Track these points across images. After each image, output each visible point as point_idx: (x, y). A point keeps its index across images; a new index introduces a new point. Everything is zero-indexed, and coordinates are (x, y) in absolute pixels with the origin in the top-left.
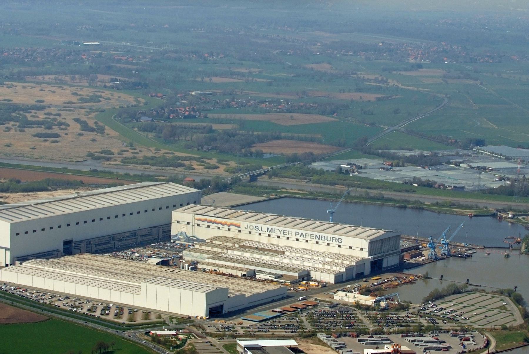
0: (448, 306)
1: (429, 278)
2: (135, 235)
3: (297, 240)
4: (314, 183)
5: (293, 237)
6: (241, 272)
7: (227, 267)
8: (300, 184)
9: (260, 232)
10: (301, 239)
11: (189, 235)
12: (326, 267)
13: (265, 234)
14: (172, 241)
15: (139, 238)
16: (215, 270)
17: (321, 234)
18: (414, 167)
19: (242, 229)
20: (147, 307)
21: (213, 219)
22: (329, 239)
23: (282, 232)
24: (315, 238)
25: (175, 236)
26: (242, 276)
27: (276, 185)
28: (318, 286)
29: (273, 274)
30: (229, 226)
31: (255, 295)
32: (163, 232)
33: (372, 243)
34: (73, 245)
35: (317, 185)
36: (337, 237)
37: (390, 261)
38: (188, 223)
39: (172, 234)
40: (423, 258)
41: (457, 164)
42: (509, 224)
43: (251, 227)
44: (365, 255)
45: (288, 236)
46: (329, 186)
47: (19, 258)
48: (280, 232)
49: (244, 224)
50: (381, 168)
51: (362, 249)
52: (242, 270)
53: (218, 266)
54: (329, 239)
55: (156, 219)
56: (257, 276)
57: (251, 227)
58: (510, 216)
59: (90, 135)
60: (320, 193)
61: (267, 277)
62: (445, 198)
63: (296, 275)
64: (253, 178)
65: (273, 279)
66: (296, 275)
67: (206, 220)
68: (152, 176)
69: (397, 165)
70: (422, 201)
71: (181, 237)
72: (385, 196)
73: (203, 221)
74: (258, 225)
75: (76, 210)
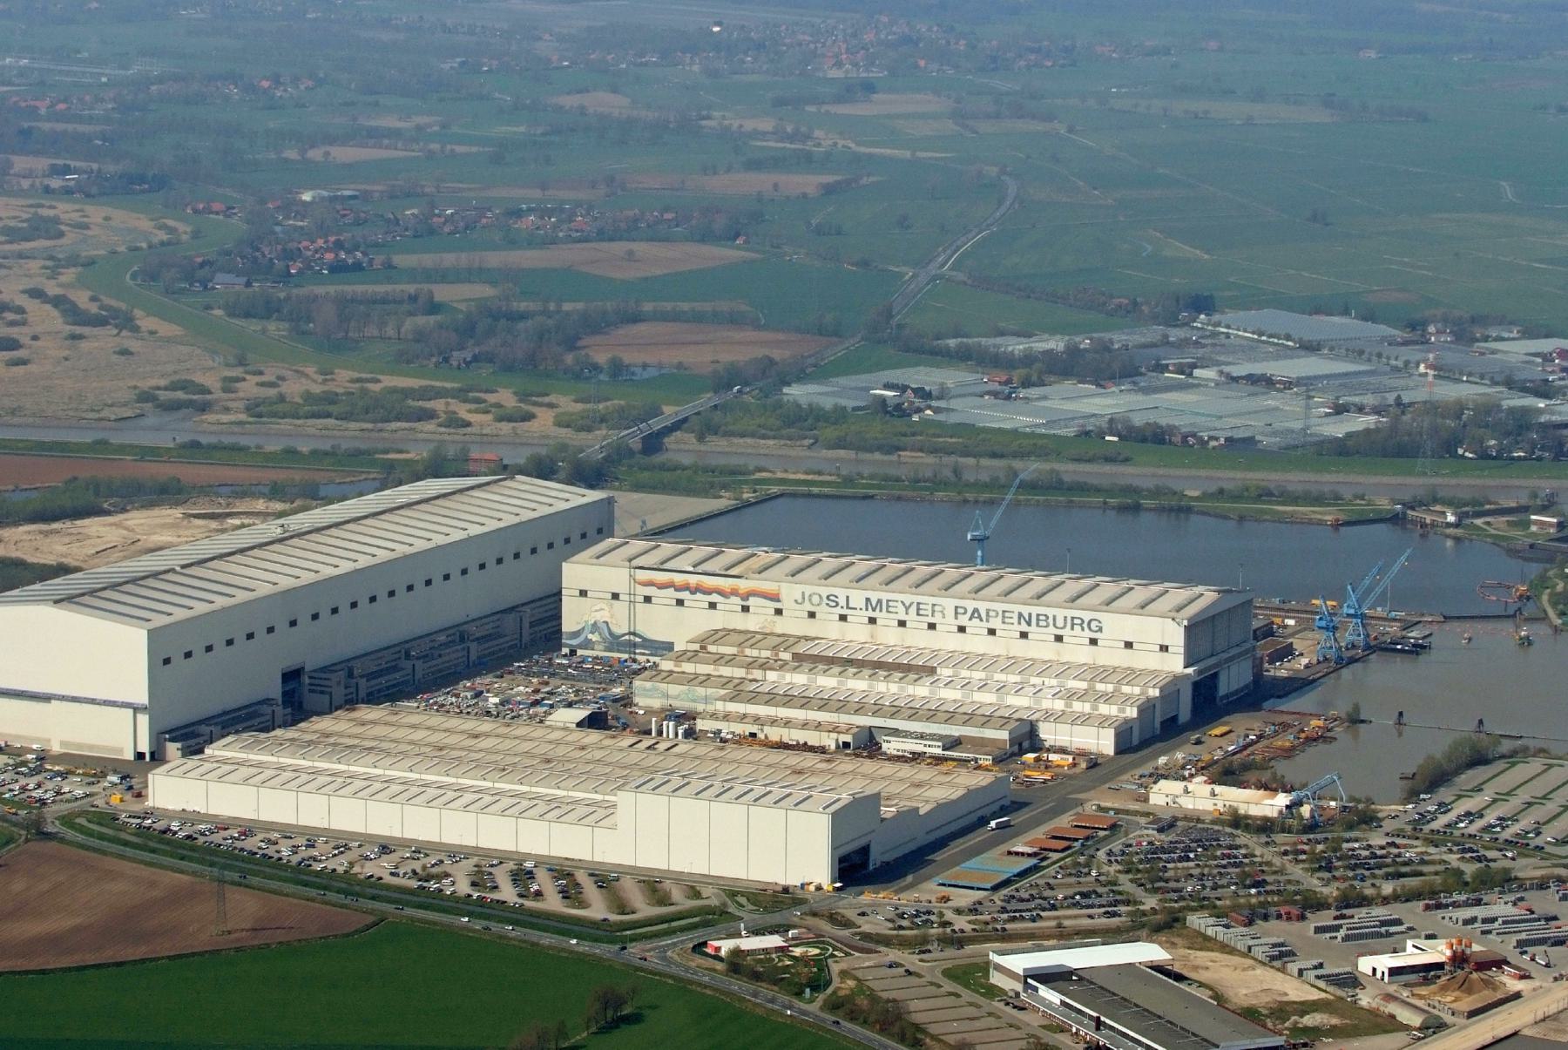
0: (1474, 803)
1: (1363, 721)
3: (962, 629)
4: (829, 448)
5: (947, 623)
6: (834, 735)
7: (787, 723)
8: (793, 453)
9: (844, 612)
10: (974, 626)
11: (620, 628)
12: (1077, 706)
13: (859, 618)
14: (565, 651)
15: (473, 646)
16: (753, 735)
17: (1035, 610)
18: (1068, 386)
21: (693, 580)
22: (1060, 623)
23: (914, 607)
24: (1015, 620)
25: (576, 634)
26: (838, 747)
27: (742, 461)
28: (1074, 765)
29: (933, 737)
30: (746, 597)
31: (941, 807)
32: (532, 625)
33: (1193, 630)
34: (307, 681)
35: (842, 453)
36: (1087, 616)
37: (1233, 679)
38: (615, 596)
39: (564, 629)
40: (1304, 661)
43: (816, 599)
44: (1175, 664)
46: (877, 456)
47: (188, 734)
48: (907, 609)
49: (790, 592)
50: (988, 393)
51: (1164, 648)
52: (835, 729)
53: (757, 720)
54: (1060, 623)
55: (512, 585)
56: (885, 746)
57: (816, 599)
59: (102, 341)
60: (872, 477)
63: (1004, 735)
64: (653, 443)
65: (939, 751)
66: (1004, 735)
69: (1026, 384)
70: (1176, 486)
71: (594, 637)
72: (1066, 478)
73: (662, 586)
74: (835, 591)
75: (307, 578)
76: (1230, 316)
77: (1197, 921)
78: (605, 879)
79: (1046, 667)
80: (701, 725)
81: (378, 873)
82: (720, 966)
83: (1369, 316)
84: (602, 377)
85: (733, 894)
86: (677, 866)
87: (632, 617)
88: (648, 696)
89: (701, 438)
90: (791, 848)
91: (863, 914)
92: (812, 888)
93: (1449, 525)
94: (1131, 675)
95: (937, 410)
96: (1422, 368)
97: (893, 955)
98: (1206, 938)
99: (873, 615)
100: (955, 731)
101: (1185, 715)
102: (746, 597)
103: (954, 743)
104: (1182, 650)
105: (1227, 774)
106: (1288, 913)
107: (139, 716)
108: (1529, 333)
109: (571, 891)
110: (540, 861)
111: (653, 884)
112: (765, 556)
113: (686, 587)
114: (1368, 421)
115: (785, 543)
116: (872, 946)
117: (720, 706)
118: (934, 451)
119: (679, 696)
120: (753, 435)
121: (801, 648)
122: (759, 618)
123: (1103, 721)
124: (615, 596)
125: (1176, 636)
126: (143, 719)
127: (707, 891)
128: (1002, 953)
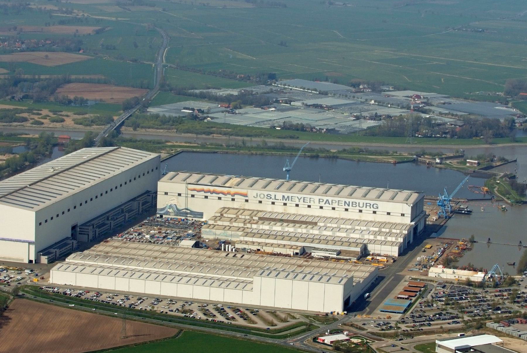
1: (475, 242)
2: (122, 212)
3: (321, 208)
4: (185, 133)
5: (315, 205)
6: (292, 250)
9: (274, 201)
11: (182, 206)
15: (127, 215)
16: (259, 250)
17: (351, 200)
18: (247, 109)
20: (162, 294)
21: (212, 188)
22: (361, 205)
23: (302, 199)
24: (343, 204)
26: (294, 254)
34: (78, 229)
36: (372, 203)
38: (179, 195)
41: (288, 102)
42: (437, 170)
45: (309, 204)
46: (204, 136)
47: (54, 252)
48: (299, 200)
49: (252, 193)
51: (403, 215)
52: (291, 247)
57: (262, 196)
58: (438, 161)
61: (327, 254)
62: (349, 143)
63: (358, 249)
65: (335, 256)
68: (15, 135)
69: (236, 108)
70: (327, 149)
71: (171, 210)
72: (286, 145)
73: (199, 191)
75: (77, 190)
76: (285, 81)
77: (490, 324)
78: (255, 311)
79: (360, 222)
80: (237, 246)
81: (165, 311)
82: (329, 348)
83: (336, 82)
84: (73, 104)
85: (307, 317)
86: (263, 304)
87: (187, 203)
88: (207, 235)
89: (135, 129)
90: (327, 298)
91: (364, 324)
92: (336, 314)
93: (437, 163)
94: (395, 225)
95: (212, 118)
96: (373, 102)
97: (391, 341)
98: (499, 332)
99: (285, 202)
100: (339, 248)
101: (411, 241)
103: (339, 253)
104: (410, 216)
105: (448, 264)
106: (521, 321)
107: (31, 246)
108: (397, 88)
109: (206, 313)
110: (225, 304)
111: (273, 312)
112: (235, 180)
113: (209, 191)
114: (371, 123)
115: (244, 173)
116: (379, 338)
117: (242, 238)
118: (225, 134)
119: (222, 235)
120: (153, 128)
121: (260, 215)
122: (239, 202)
123: (392, 244)
124: (179, 195)
125: (408, 210)
126: (33, 247)
127: (298, 316)
128: (441, 340)
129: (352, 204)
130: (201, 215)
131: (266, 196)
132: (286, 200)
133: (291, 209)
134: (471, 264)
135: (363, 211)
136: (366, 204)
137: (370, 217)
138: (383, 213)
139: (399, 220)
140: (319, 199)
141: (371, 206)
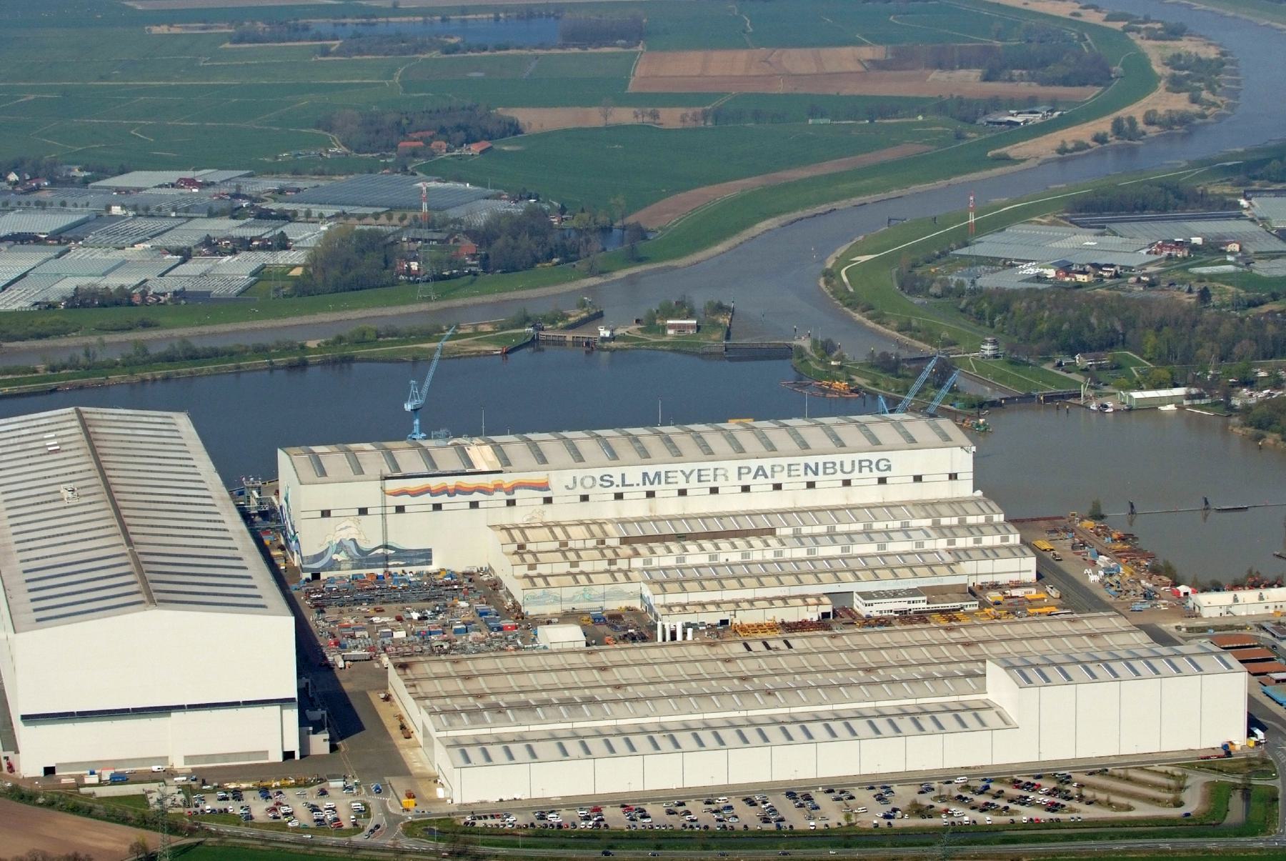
3: (746, 489)
5: (730, 486)
10: (761, 486)
11: (371, 539)
16: (724, 622)
19: (556, 492)
22: (847, 468)
23: (695, 473)
25: (318, 557)
30: (511, 490)
38: (363, 511)
45: (714, 485)
48: (687, 477)
49: (560, 480)
51: (953, 477)
57: (588, 482)
61: (901, 604)
65: (923, 606)
67: (427, 490)
71: (341, 557)
102: (511, 490)
104: (971, 476)
113: (444, 491)
124: (363, 511)
125: (961, 459)
126: (292, 715)
129: (825, 468)
130: (426, 556)
131: (599, 482)
132: (652, 483)
133: (668, 505)
134: (1254, 572)
135: (853, 483)
136: (860, 462)
137: (874, 494)
138: (932, 478)
139: (940, 490)
140: (740, 468)
141: (873, 466)
